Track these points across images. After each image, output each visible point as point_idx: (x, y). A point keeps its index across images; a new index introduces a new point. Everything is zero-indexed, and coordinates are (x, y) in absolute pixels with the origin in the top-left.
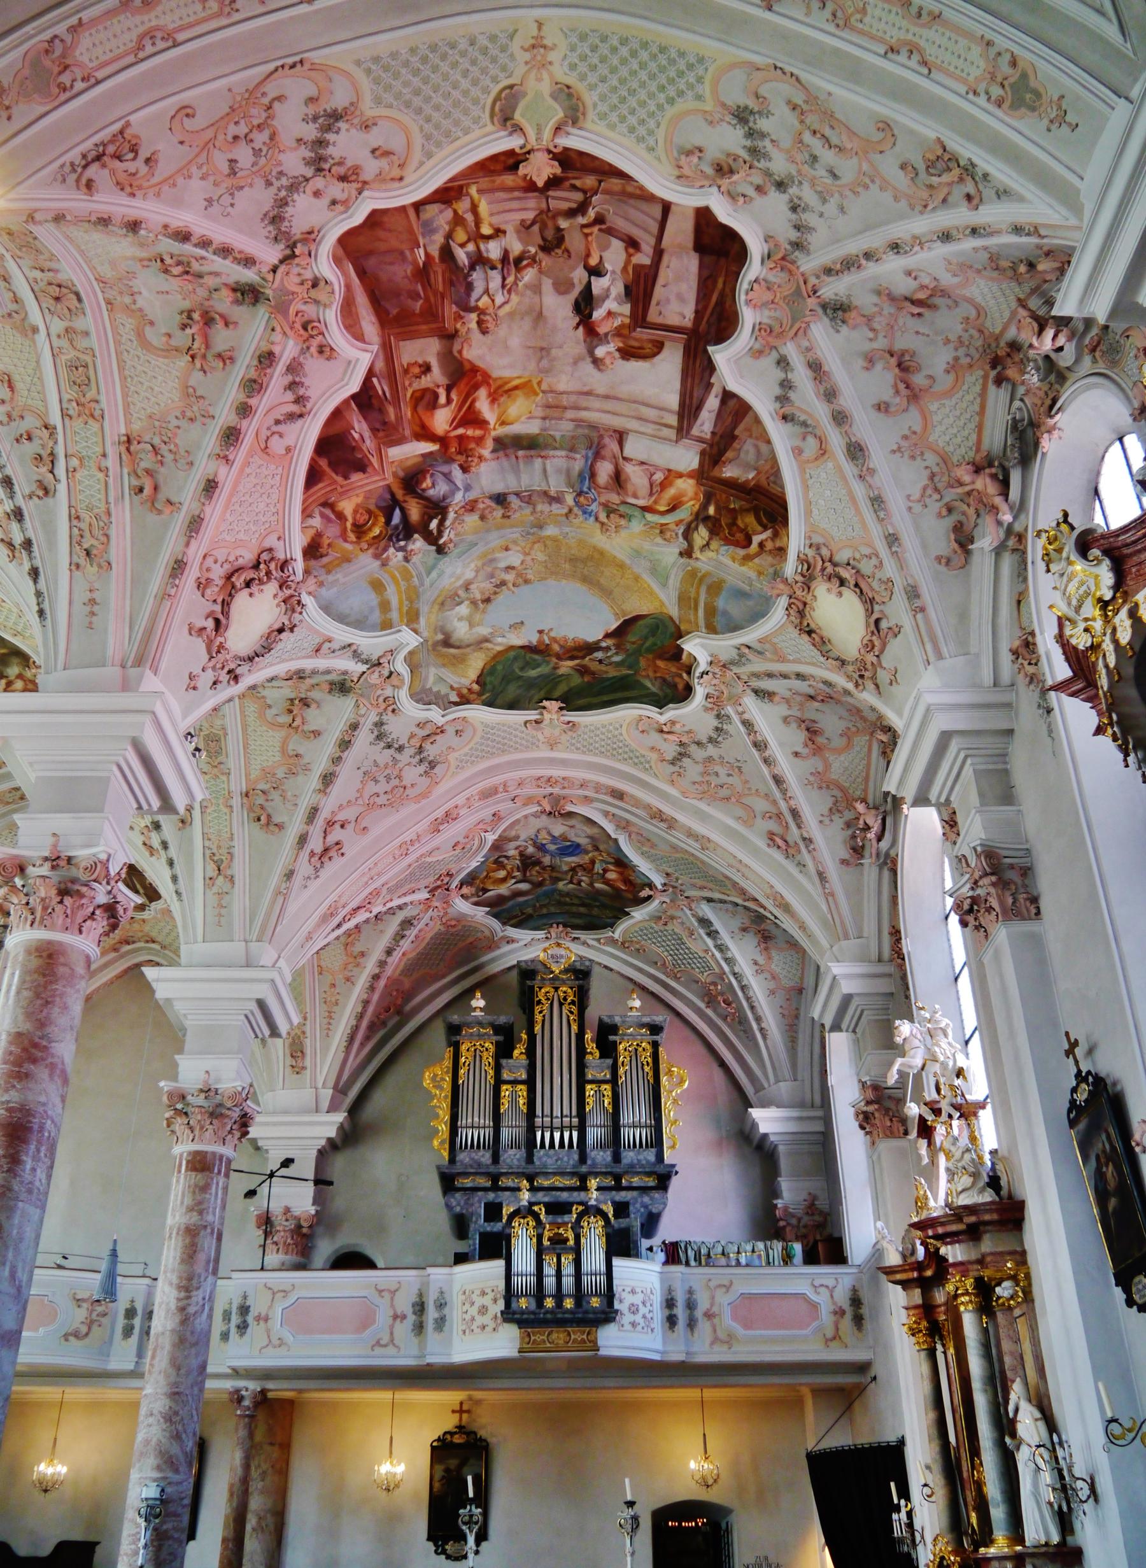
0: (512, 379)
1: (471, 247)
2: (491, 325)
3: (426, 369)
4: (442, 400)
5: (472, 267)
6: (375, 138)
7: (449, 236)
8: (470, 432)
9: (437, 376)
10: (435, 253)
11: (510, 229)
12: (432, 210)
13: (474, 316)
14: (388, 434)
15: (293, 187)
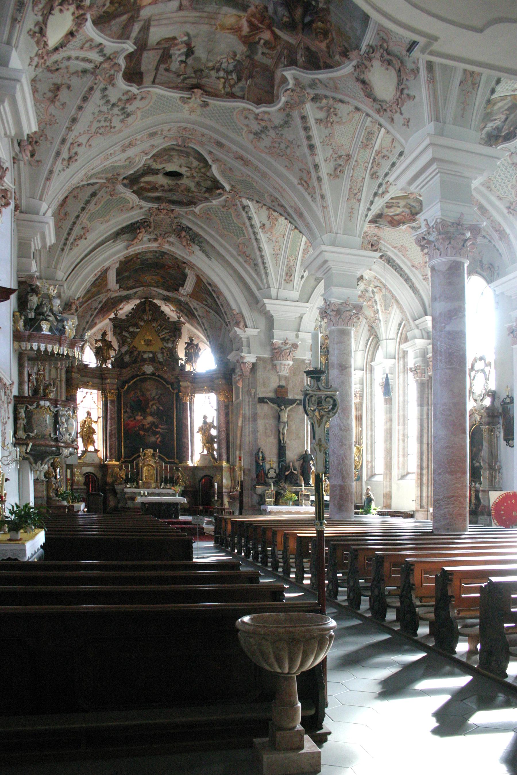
0: (230, 33)
1: (230, 77)
2: (231, 54)
3: (263, 54)
4: (262, 42)
5: (232, 72)
6: (246, 122)
7: (236, 83)
8: (256, 22)
9: (260, 49)
10: (243, 80)
11: (214, 78)
12: (239, 94)
13: (237, 58)
14: (289, 46)
15: (276, 127)
